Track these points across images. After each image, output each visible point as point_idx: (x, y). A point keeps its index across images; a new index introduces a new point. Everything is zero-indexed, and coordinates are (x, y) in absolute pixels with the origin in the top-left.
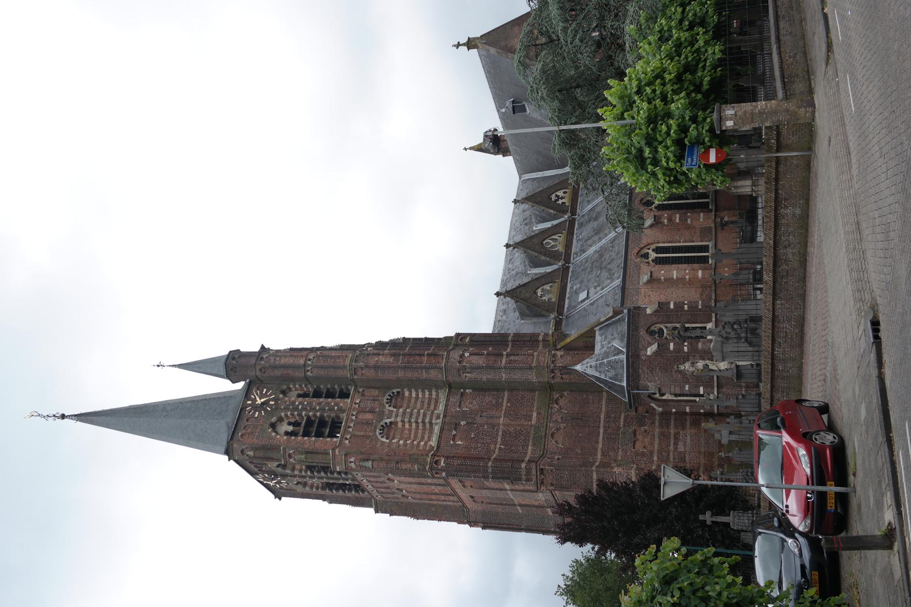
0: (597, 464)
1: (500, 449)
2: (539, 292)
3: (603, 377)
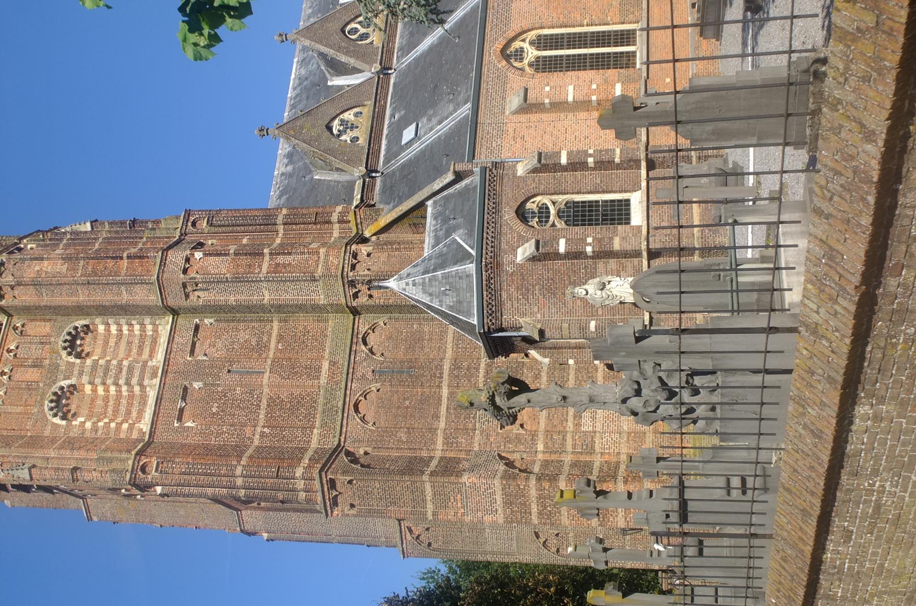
0: (434, 463)
1: (262, 435)
2: (336, 126)
3: (436, 305)
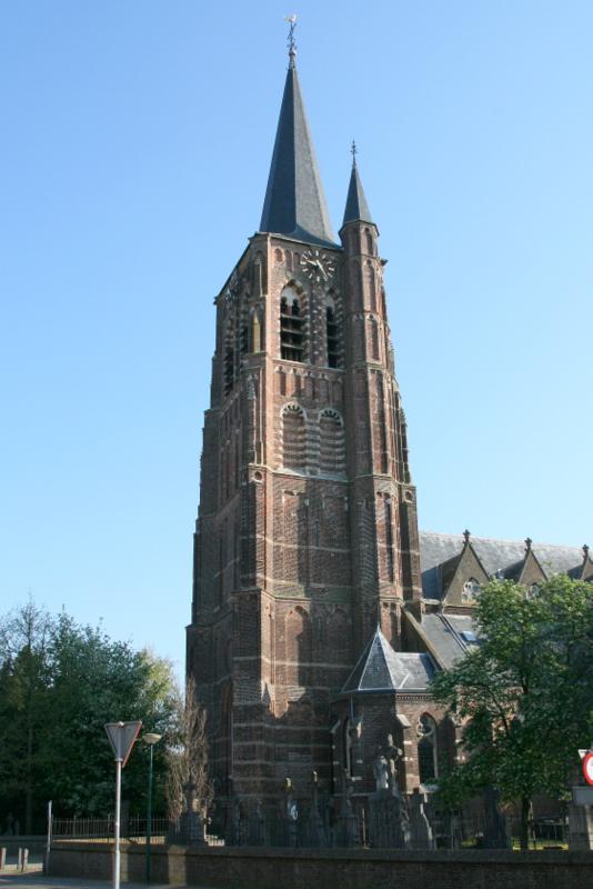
3: (368, 663)
